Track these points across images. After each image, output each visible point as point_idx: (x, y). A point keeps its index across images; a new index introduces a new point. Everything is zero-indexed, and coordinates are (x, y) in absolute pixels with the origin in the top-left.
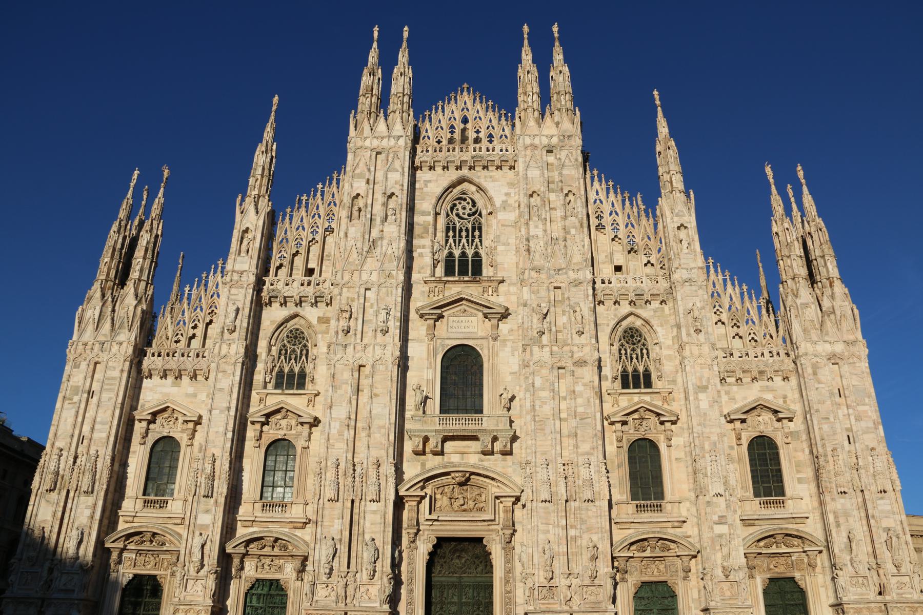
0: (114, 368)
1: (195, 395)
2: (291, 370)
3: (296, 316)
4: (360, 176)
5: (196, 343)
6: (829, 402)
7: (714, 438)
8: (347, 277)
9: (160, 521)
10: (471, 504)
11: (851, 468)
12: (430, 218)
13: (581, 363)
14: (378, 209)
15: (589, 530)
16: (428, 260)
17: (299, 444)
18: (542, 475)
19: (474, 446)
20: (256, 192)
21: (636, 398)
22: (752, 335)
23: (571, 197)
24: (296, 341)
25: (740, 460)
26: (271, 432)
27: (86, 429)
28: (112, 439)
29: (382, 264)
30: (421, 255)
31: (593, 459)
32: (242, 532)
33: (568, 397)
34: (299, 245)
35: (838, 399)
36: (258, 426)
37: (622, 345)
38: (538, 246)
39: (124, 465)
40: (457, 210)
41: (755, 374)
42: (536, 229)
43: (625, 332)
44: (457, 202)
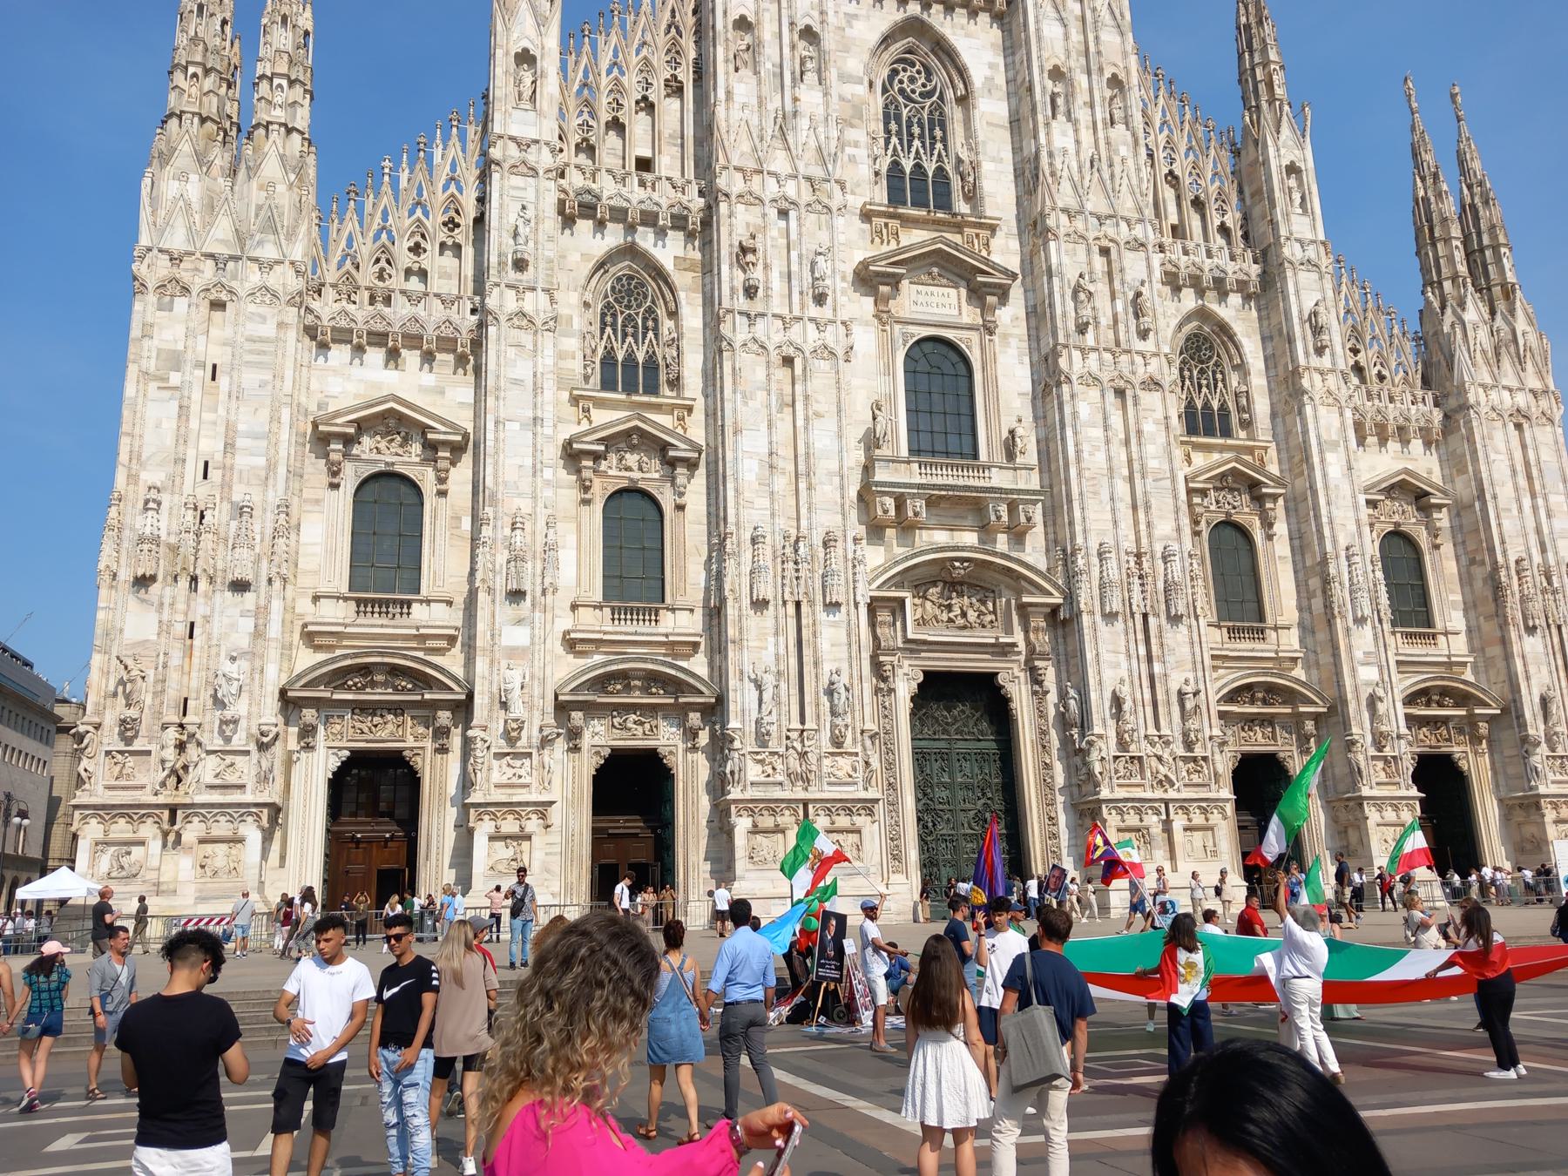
0: (264, 319)
6: (1510, 485)
9: (399, 644)
10: (972, 615)
11: (1544, 591)
12: (862, 90)
13: (1153, 384)
15: (1179, 664)
16: (865, 171)
22: (1379, 367)
26: (610, 472)
27: (211, 446)
28: (282, 470)
29: (807, 165)
30: (852, 159)
33: (1133, 441)
35: (1522, 481)
36: (588, 463)
37: (1183, 362)
40: (901, 82)
43: (1188, 339)
44: (900, 67)
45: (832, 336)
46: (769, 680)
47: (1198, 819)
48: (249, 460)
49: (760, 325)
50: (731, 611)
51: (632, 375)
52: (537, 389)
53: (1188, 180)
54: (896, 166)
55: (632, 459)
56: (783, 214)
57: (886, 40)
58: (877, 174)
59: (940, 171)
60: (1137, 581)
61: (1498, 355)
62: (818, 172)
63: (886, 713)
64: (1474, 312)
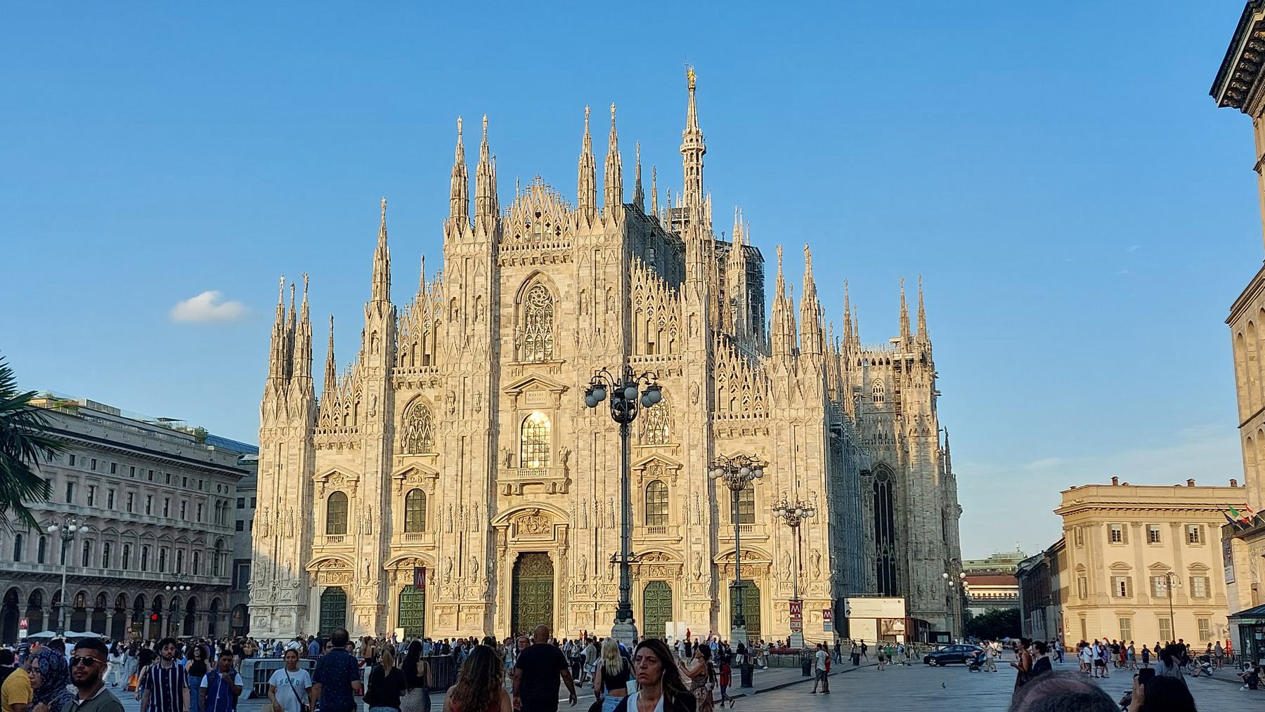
4: (455, 281)
5: (350, 420)
7: (699, 483)
8: (450, 369)
10: (541, 528)
12: (512, 310)
14: (470, 310)
16: (511, 346)
17: (428, 492)
18: (581, 511)
20: (378, 298)
21: (654, 451)
23: (612, 293)
24: (420, 414)
27: (281, 492)
31: (615, 499)
32: (395, 555)
39: (311, 513)
42: (585, 323)
60: (593, 514)
64: (782, 371)
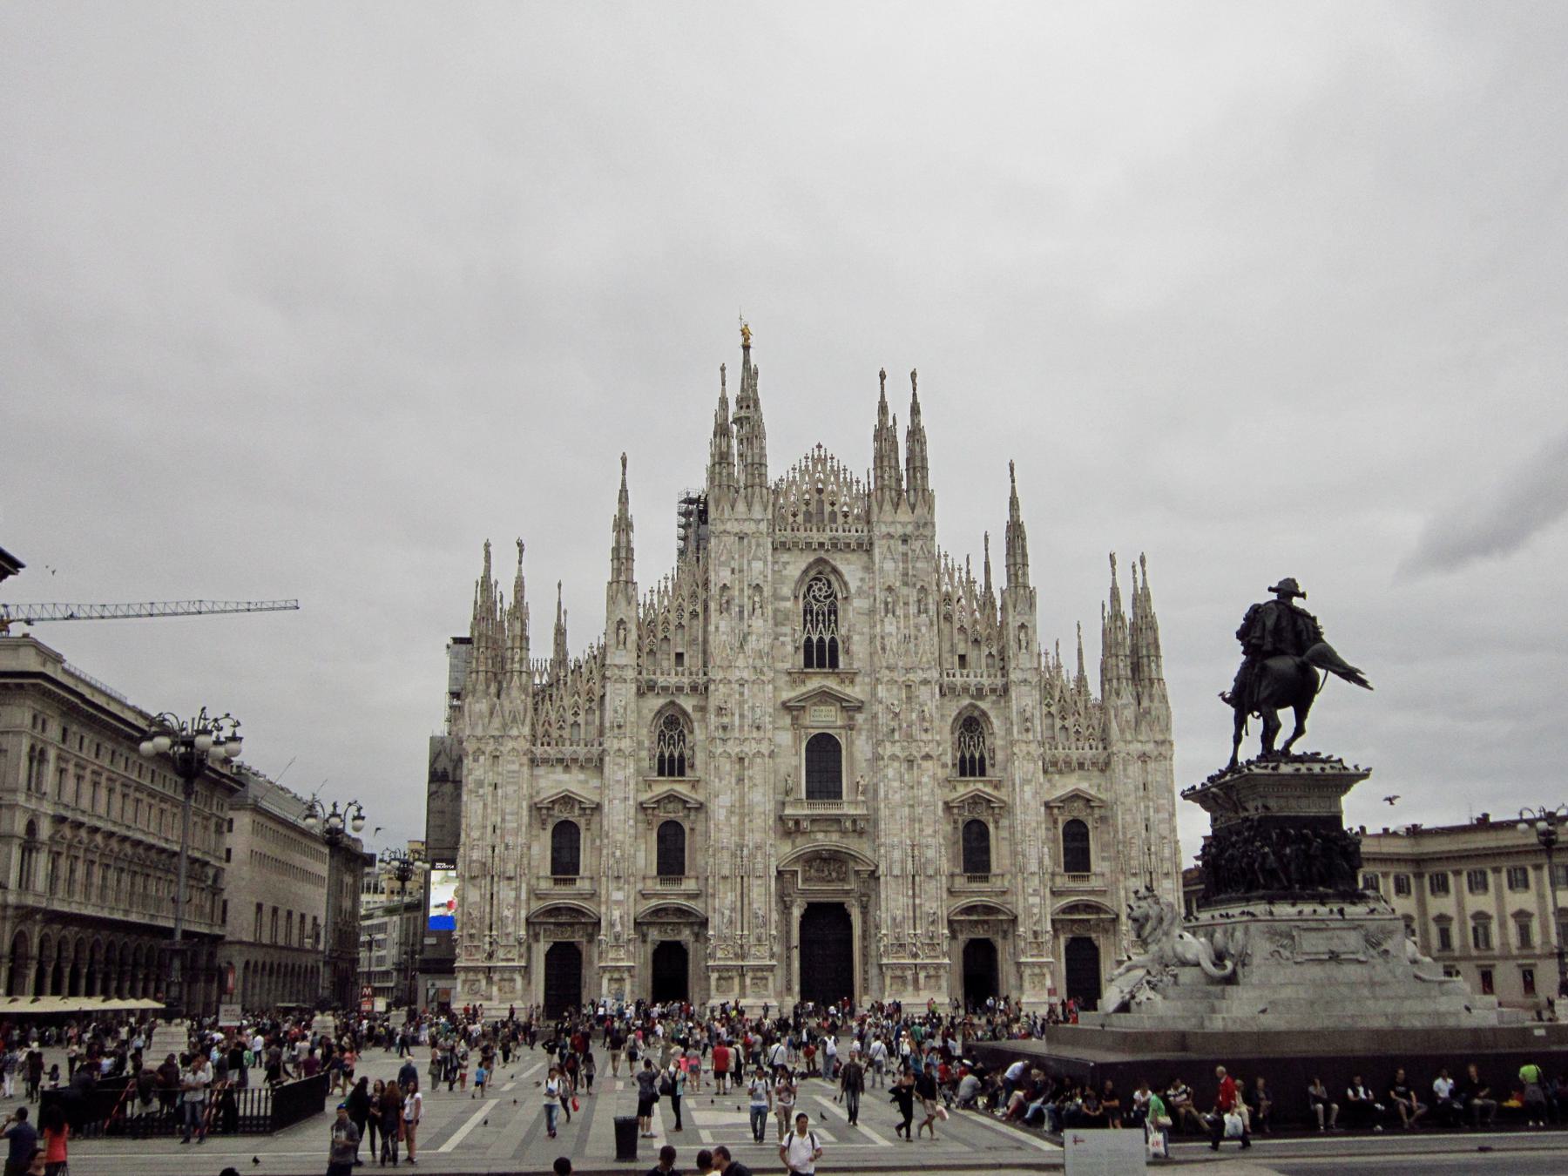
1: (586, 782)
2: (671, 755)
3: (672, 703)
7: (1034, 825)
10: (834, 875)
13: (927, 757)
16: (790, 648)
19: (835, 827)
20: (623, 578)
21: (972, 787)
25: (1055, 840)
30: (783, 643)
34: (665, 630)
35: (1141, 793)
38: (891, 643)
41: (1075, 764)
45: (765, 748)
46: (727, 913)
47: (932, 972)
48: (511, 825)
49: (730, 743)
50: (711, 881)
51: (672, 766)
52: (627, 784)
53: (970, 631)
54: (809, 640)
55: (670, 806)
56: (742, 685)
57: (805, 572)
58: (797, 649)
59: (833, 640)
61: (1137, 723)
62: (759, 663)
63: (788, 924)
64: (1127, 696)
